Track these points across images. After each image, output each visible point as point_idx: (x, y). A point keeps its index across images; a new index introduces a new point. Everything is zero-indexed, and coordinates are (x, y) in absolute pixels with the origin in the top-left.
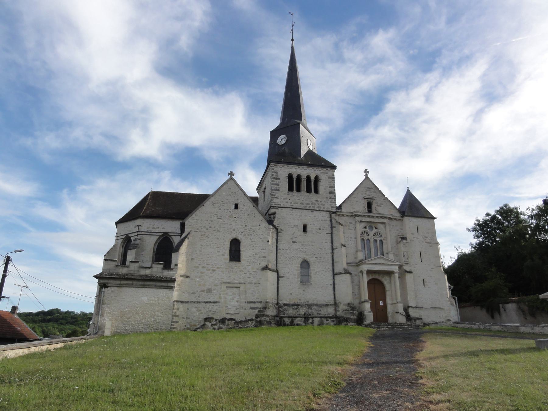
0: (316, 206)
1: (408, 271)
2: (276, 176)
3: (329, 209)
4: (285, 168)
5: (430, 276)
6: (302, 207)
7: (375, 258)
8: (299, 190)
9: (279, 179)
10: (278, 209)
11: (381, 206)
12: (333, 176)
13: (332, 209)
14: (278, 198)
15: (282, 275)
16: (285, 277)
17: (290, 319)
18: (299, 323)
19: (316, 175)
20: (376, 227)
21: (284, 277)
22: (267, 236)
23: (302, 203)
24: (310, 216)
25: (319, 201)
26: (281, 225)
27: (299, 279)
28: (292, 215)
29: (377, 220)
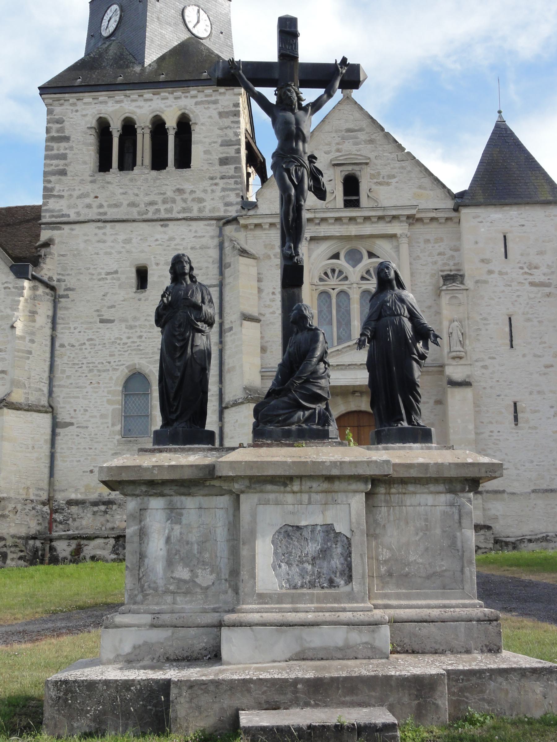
0: (178, 206)
1: (460, 380)
2: (58, 131)
3: (219, 210)
4: (85, 104)
5: (539, 392)
6: (134, 213)
7: (340, 347)
8: (45, 165)
9: (67, 139)
10: (60, 229)
11: (388, 184)
12: (234, 109)
13: (225, 211)
14: (61, 197)
15: (68, 420)
16: (76, 426)
17: (74, 543)
18: (99, 552)
19: (179, 113)
20: (371, 250)
21: (72, 424)
22: (9, 311)
23: (133, 204)
24: (157, 240)
25: (188, 191)
26: (68, 275)
27: (118, 427)
28: (104, 242)
29: (368, 229)
